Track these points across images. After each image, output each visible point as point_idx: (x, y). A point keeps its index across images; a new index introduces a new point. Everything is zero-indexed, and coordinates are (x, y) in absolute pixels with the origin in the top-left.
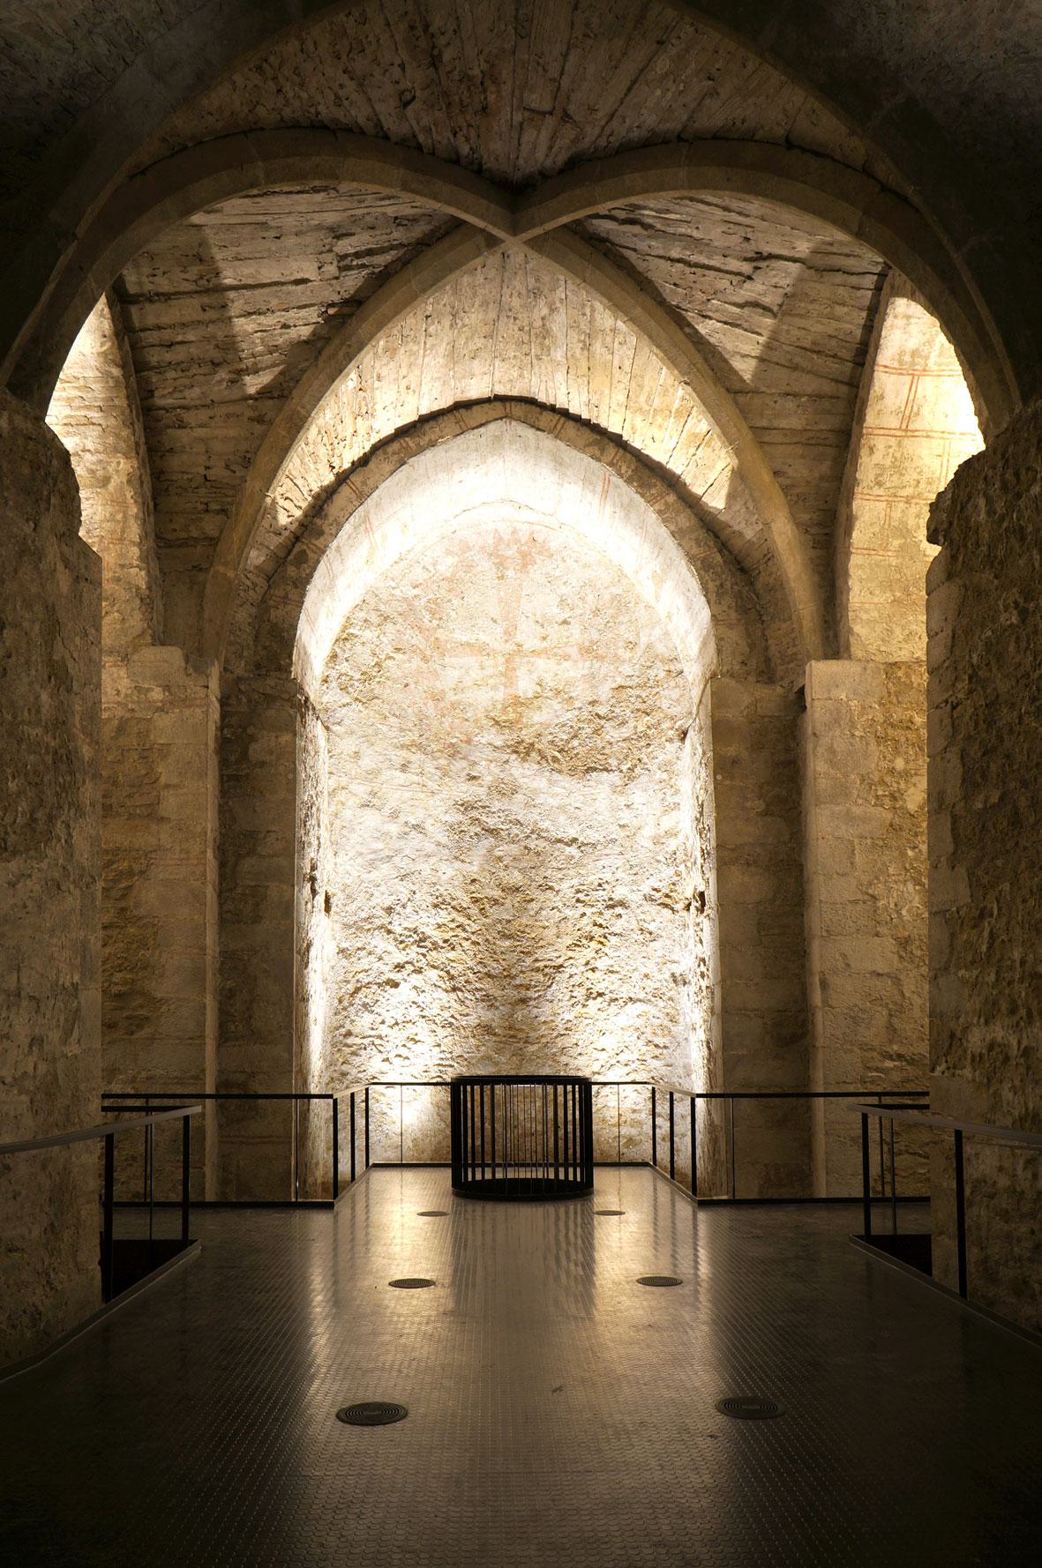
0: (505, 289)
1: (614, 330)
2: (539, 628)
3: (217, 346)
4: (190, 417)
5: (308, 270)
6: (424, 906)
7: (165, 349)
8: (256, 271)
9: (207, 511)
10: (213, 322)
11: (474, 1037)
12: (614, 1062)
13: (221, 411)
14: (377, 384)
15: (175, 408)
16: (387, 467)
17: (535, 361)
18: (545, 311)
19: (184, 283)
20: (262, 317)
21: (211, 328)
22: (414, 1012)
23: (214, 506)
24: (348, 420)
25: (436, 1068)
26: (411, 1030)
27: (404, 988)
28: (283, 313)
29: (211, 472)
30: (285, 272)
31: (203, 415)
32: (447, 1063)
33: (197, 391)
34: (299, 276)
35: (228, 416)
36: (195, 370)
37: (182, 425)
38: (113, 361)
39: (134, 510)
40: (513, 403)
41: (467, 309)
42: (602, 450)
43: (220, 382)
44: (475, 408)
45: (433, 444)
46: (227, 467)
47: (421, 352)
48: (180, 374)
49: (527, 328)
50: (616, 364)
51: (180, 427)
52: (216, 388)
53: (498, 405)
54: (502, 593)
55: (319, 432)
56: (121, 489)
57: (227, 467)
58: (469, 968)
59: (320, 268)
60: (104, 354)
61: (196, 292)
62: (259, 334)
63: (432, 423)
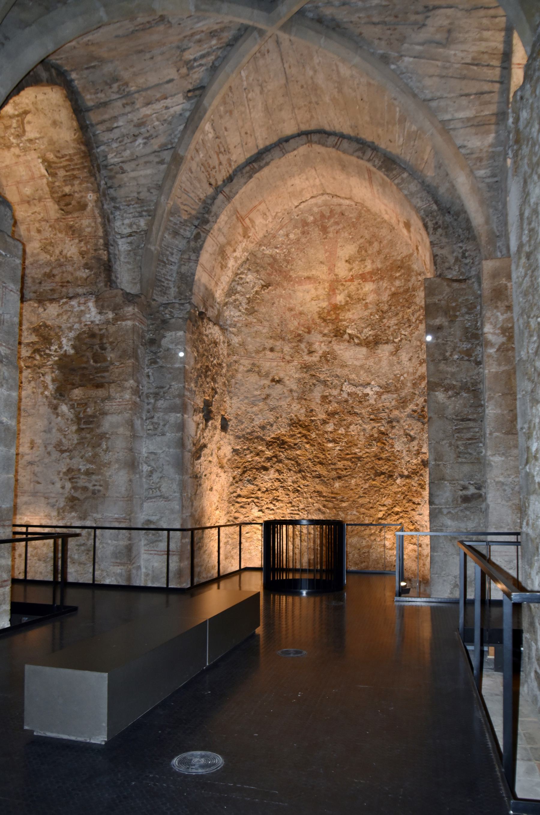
1: (352, 76)
2: (347, 264)
3: (135, 126)
4: (126, 167)
6: (283, 425)
7: (109, 133)
8: (146, 80)
10: (129, 113)
11: (311, 498)
12: (389, 512)
13: (142, 161)
14: (226, 133)
15: (118, 163)
16: (243, 180)
17: (316, 106)
18: (311, 73)
21: (130, 116)
22: (277, 484)
24: (215, 157)
25: (289, 515)
26: (276, 494)
27: (272, 471)
28: (165, 101)
29: (141, 194)
31: (133, 165)
32: (296, 512)
33: (128, 153)
35: (146, 163)
38: (82, 142)
40: (312, 135)
42: (364, 153)
43: (139, 145)
44: (291, 141)
45: (267, 164)
46: (149, 191)
47: (248, 111)
49: (305, 86)
50: (359, 98)
51: (123, 173)
52: (137, 149)
53: (304, 137)
54: (326, 247)
55: (198, 165)
56: (93, 210)
58: (309, 459)
61: (119, 98)
62: (155, 115)
63: (267, 153)
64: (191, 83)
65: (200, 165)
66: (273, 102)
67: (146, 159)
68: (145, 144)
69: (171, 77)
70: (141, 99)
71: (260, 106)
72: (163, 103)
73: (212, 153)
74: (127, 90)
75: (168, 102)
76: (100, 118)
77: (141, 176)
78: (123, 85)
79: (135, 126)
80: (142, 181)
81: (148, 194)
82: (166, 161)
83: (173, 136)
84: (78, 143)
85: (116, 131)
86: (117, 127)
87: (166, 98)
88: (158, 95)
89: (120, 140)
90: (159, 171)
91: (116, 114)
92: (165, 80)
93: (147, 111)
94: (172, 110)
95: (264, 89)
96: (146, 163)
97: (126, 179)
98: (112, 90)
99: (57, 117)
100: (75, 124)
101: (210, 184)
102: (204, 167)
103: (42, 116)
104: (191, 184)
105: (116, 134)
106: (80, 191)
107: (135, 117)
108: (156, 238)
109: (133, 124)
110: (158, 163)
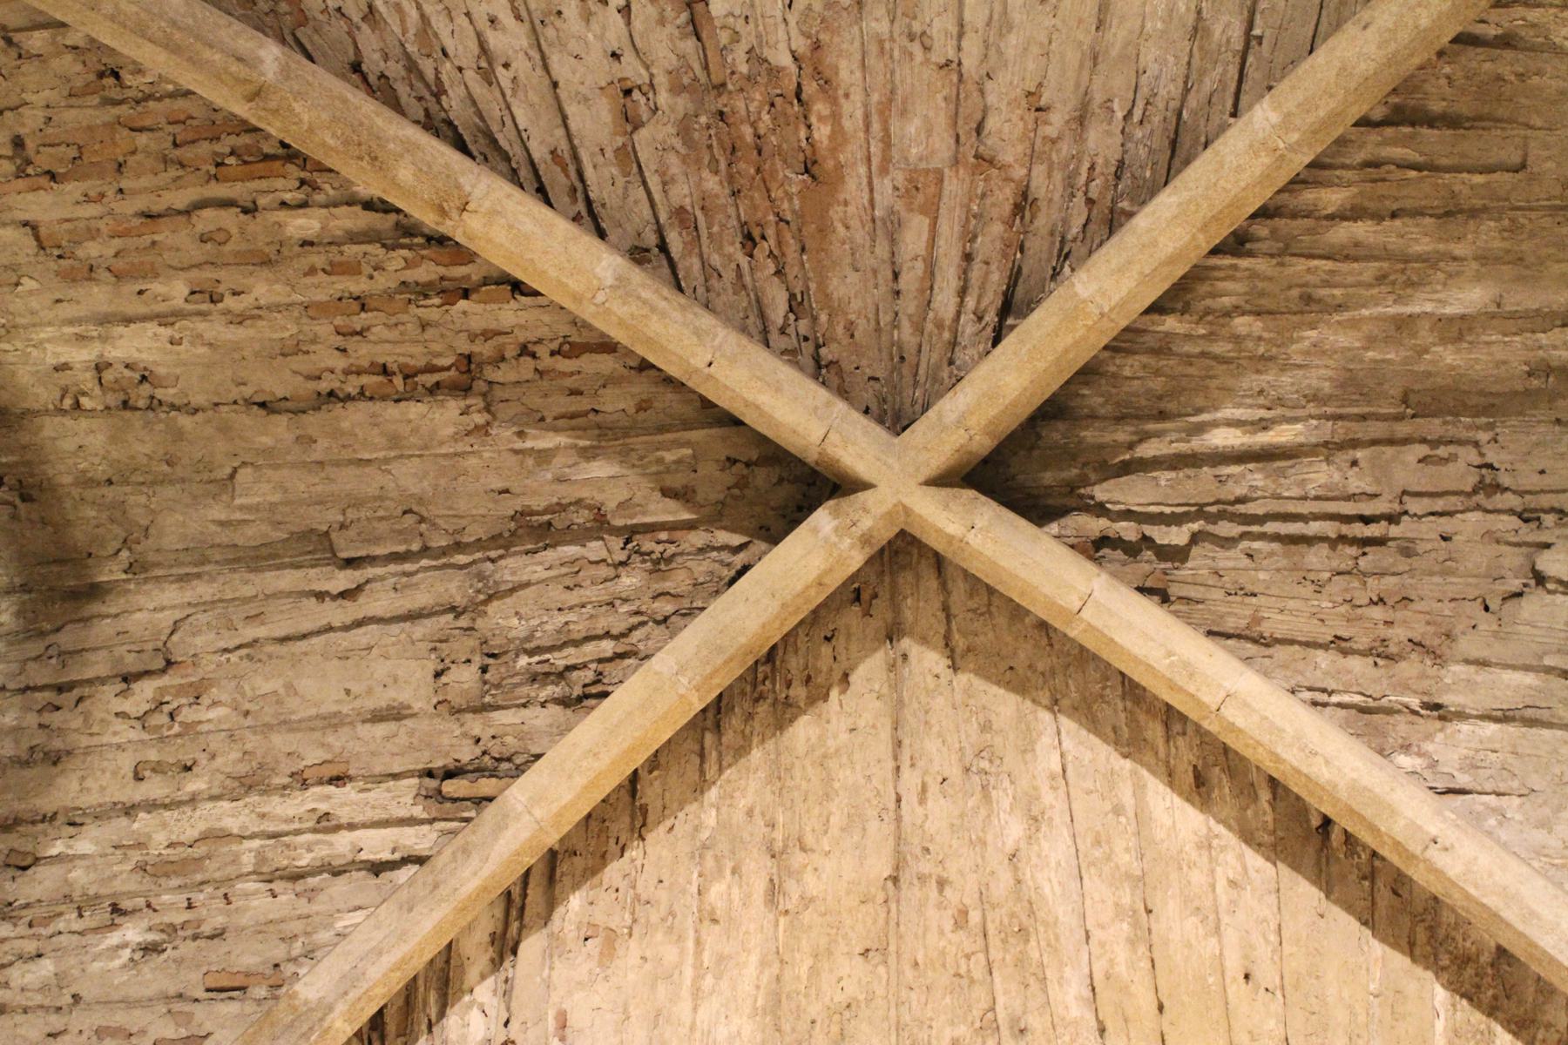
0: (906, 772)
3: (142, 868)
5: (413, 686)
8: (289, 687)
10: (152, 806)
18: (1015, 830)
19: (120, 725)
20: (276, 799)
21: (143, 821)
30: (356, 688)
33: (47, 967)
34: (381, 700)
36: (70, 921)
41: (809, 840)
47: (689, 972)
48: (22, 929)
49: (975, 917)
50: (1234, 966)
52: (97, 965)
59: (438, 675)
62: (256, 843)
66: (814, 971)
67: (120, 1018)
68: (149, 949)
69: (404, 695)
70: (229, 760)
71: (749, 977)
72: (318, 799)
74: (187, 715)
75: (344, 801)
78: (180, 690)
79: (142, 868)
83: (297, 948)
85: (41, 872)
86: (59, 858)
87: (338, 780)
88: (313, 756)
91: (89, 800)
92: (370, 704)
93: (231, 816)
94: (342, 844)
95: (791, 886)
98: (127, 706)
105: (39, 885)
109: (136, 856)
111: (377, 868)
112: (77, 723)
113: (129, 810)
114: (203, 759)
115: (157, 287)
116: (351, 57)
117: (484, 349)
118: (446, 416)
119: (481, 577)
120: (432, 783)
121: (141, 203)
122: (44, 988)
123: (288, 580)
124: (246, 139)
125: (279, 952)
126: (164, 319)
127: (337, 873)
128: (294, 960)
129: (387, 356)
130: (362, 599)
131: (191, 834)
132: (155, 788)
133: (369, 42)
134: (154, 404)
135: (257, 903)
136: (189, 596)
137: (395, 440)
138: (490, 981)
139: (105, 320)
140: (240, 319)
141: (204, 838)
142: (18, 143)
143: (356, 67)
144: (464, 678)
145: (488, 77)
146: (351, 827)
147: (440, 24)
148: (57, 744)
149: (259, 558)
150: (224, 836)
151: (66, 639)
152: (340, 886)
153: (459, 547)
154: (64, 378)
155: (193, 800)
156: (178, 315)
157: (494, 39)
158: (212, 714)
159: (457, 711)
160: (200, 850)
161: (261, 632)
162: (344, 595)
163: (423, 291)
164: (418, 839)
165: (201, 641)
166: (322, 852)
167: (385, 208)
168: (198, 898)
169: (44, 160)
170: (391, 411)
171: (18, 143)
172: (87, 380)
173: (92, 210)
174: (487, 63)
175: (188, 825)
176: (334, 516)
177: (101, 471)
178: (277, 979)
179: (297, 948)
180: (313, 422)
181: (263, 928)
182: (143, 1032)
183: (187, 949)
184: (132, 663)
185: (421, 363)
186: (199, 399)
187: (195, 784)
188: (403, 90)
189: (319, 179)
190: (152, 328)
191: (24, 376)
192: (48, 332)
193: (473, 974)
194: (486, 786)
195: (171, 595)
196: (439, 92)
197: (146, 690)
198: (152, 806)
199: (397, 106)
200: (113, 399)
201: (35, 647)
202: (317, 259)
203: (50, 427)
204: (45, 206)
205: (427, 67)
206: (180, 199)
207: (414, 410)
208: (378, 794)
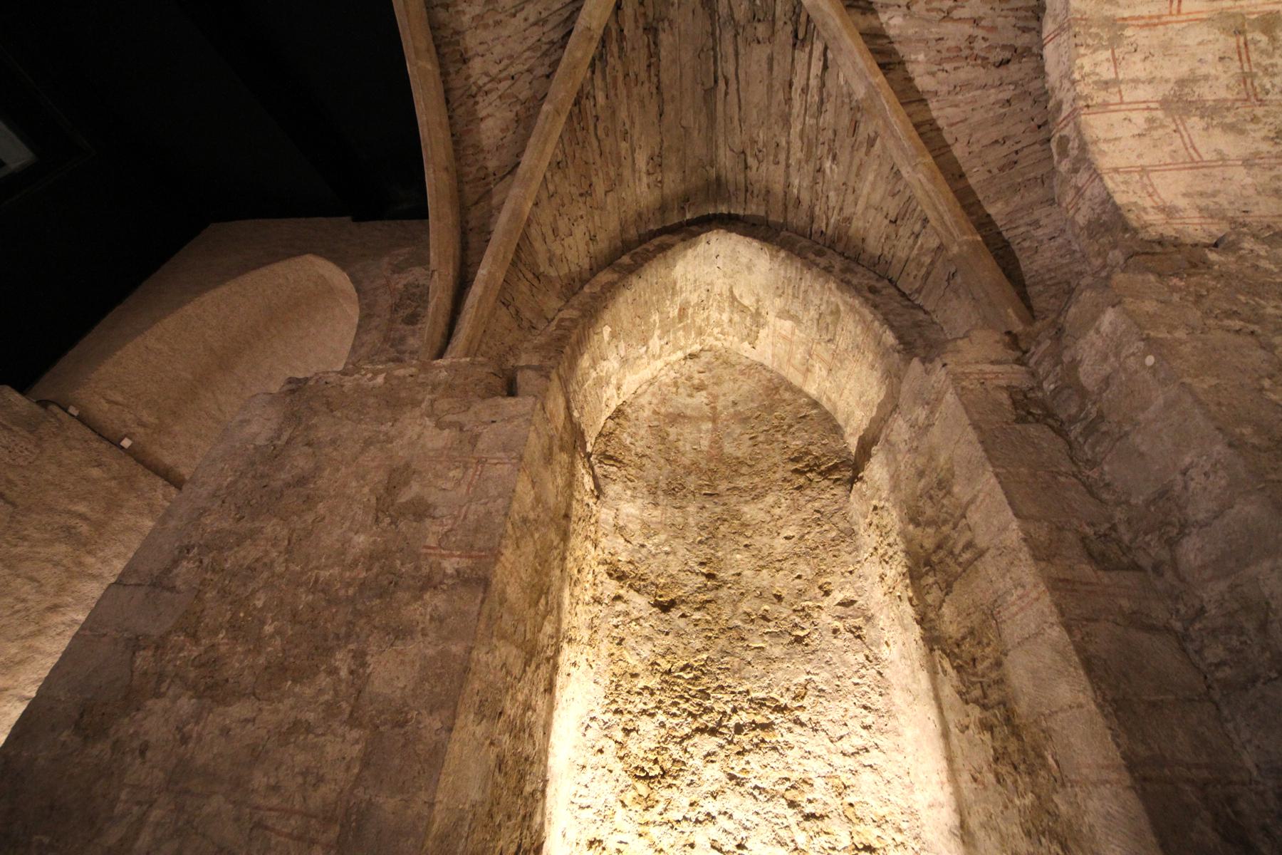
3: (807, 161)
4: (847, 213)
8: (755, 107)
9: (917, 236)
10: (788, 158)
19: (760, 171)
21: (792, 161)
23: (917, 228)
29: (890, 214)
30: (760, 79)
31: (850, 198)
33: (832, 194)
34: (765, 66)
35: (858, 175)
37: (848, 220)
39: (857, 303)
48: (818, 203)
52: (835, 177)
55: (933, 74)
56: (845, 303)
57: (894, 195)
59: (759, 42)
60: (771, 255)
64: (785, 23)
65: (935, 68)
67: (854, 168)
68: (834, 158)
69: (765, 57)
70: (777, 129)
72: (796, 94)
73: (935, 31)
75: (798, 82)
76: (780, 206)
77: (869, 194)
78: (752, 149)
80: (876, 198)
81: (897, 197)
82: (872, 135)
84: (777, 257)
85: (801, 197)
87: (791, 85)
88: (781, 96)
89: (816, 196)
90: (879, 156)
91: (782, 180)
92: (766, 72)
93: (796, 128)
96: (858, 175)
97: (861, 224)
98: (754, 169)
99: (744, 260)
100: (756, 244)
101: (1004, 63)
102: (949, 59)
103: (738, 275)
104: (956, 106)
105: (806, 197)
106: (821, 299)
107: (797, 154)
108: (947, 229)
110: (867, 153)
111: (825, 67)
112: (757, 186)
113: (788, 166)
114: (776, 139)
115: (623, 152)
116: (544, 79)
117: (641, 22)
118: (666, 39)
119: (725, 23)
120: (799, 42)
121: (597, 157)
122: (838, 195)
123: (720, 107)
124: (575, 119)
125: (847, 108)
126: (633, 151)
127: (823, 85)
128: (851, 101)
129: (644, 63)
130: (729, 76)
131: (799, 144)
132: (782, 157)
133: (541, 71)
134: (660, 156)
135: (828, 118)
136: (722, 146)
137: (674, 61)
138: (880, 15)
139: (634, 171)
140: (633, 123)
141: (801, 138)
142: (581, 195)
143: (548, 76)
144: (761, 30)
145: (545, 21)
146: (808, 79)
147: (530, 42)
148: (763, 192)
149: (712, 118)
150: (802, 130)
151: (732, 189)
152: (829, 84)
153: (713, 34)
154: (652, 186)
155: (788, 143)
156: (632, 145)
157: (532, 20)
158: (761, 135)
159: (773, 33)
160: (805, 140)
161: (736, 117)
162: (727, 84)
163: (621, 49)
164: (818, 48)
165: (737, 140)
166: (815, 90)
167: (592, 65)
168: (821, 140)
169: (586, 188)
170: (663, 63)
171: (581, 195)
172: (652, 178)
173: (600, 174)
174: (541, 22)
175: (796, 144)
176: (699, 88)
177: (680, 175)
178: (856, 109)
179: (847, 100)
180: (666, 96)
181: (837, 115)
182: (861, 160)
183: (837, 144)
184: (742, 166)
185: (646, 50)
186: (659, 139)
187: (784, 143)
188: (554, 58)
189: (585, 92)
190: (636, 155)
191: (651, 198)
192: (638, 190)
193: (875, 23)
194: (803, 19)
195: (721, 152)
196: (552, 43)
197: (751, 161)
198: (788, 158)
199: (558, 61)
200: (658, 170)
201: (734, 199)
202: (612, 93)
203: (667, 191)
204: (600, 188)
205: (545, 47)
206: (595, 143)
207: (663, 53)
208: (798, 68)
